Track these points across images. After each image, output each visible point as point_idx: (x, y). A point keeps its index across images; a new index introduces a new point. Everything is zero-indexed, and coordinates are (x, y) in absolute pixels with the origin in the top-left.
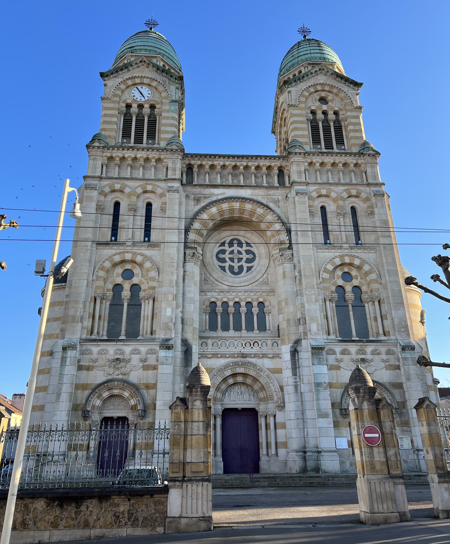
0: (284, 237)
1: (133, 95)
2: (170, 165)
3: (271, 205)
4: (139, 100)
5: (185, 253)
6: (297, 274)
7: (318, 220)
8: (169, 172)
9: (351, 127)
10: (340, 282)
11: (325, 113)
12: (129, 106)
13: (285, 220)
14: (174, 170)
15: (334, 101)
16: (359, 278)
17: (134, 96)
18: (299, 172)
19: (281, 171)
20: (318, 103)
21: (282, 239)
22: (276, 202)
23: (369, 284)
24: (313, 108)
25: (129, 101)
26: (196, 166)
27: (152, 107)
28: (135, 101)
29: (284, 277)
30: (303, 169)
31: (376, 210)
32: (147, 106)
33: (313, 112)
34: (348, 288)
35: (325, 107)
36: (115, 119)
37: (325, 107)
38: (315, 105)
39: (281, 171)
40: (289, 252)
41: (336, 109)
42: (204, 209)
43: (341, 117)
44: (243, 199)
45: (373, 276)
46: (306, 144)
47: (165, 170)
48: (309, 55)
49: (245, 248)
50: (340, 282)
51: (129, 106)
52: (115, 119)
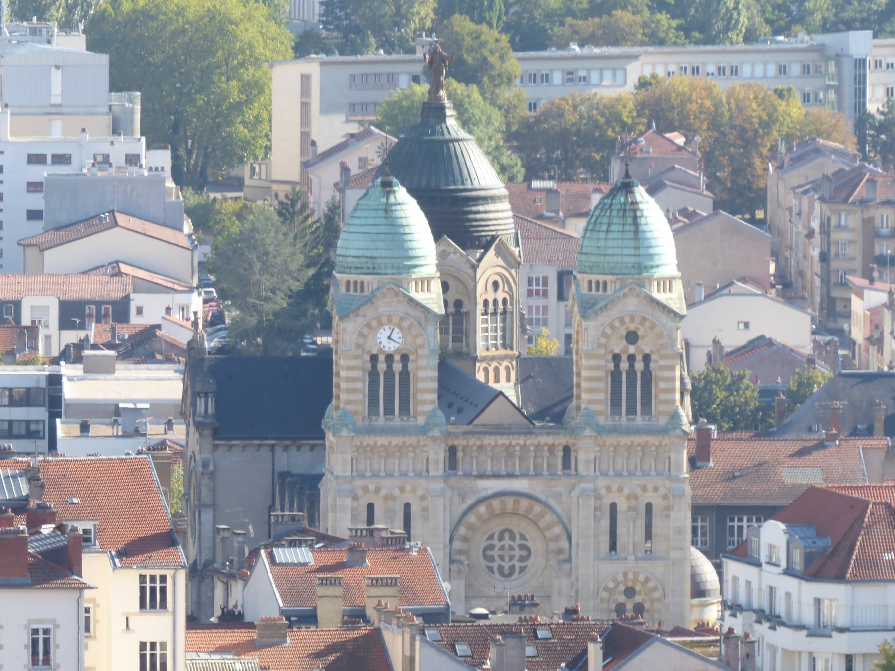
0: (564, 544)
1: (379, 341)
2: (431, 457)
3: (552, 502)
4: (387, 349)
5: (450, 570)
6: (573, 594)
7: (605, 524)
8: (431, 467)
9: (662, 385)
10: (622, 599)
11: (632, 358)
12: (374, 358)
13: (566, 521)
14: (437, 463)
15: (646, 339)
16: (643, 594)
17: (381, 343)
18: (587, 462)
19: (567, 450)
20: (624, 343)
21: (561, 547)
22: (558, 496)
23: (652, 602)
24: (617, 351)
25: (375, 352)
26: (460, 449)
27: (405, 358)
28: (381, 351)
29: (560, 595)
30: (592, 457)
31: (672, 514)
32: (397, 358)
33: (616, 358)
34: (630, 606)
35: (632, 349)
36: (359, 385)
37: (632, 349)
38: (618, 346)
39: (567, 450)
40: (567, 566)
41: (647, 351)
42: (472, 508)
43: (652, 365)
44: (518, 495)
45: (657, 595)
46: (600, 413)
47: (425, 461)
48: (619, 259)
49: (518, 565)
50: (622, 599)
51: (374, 358)
52: (359, 385)
